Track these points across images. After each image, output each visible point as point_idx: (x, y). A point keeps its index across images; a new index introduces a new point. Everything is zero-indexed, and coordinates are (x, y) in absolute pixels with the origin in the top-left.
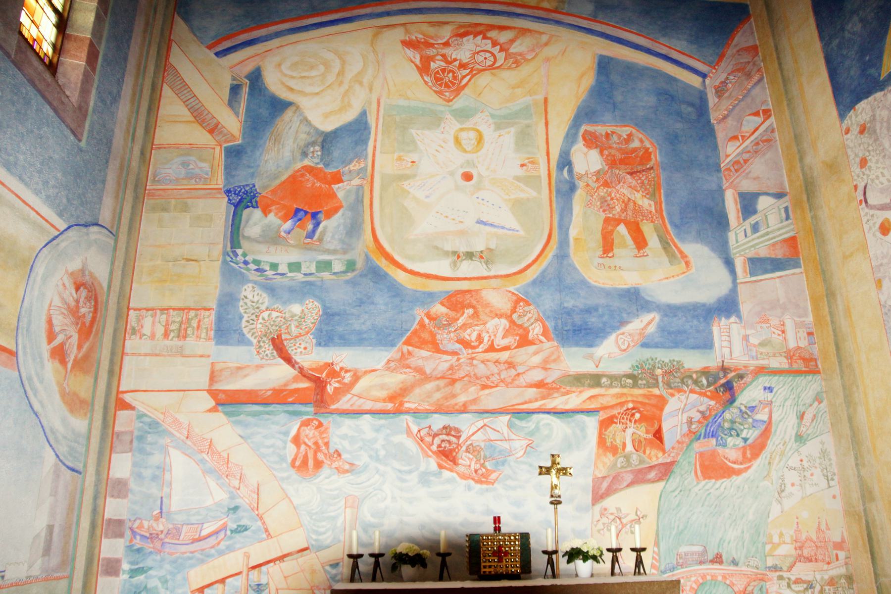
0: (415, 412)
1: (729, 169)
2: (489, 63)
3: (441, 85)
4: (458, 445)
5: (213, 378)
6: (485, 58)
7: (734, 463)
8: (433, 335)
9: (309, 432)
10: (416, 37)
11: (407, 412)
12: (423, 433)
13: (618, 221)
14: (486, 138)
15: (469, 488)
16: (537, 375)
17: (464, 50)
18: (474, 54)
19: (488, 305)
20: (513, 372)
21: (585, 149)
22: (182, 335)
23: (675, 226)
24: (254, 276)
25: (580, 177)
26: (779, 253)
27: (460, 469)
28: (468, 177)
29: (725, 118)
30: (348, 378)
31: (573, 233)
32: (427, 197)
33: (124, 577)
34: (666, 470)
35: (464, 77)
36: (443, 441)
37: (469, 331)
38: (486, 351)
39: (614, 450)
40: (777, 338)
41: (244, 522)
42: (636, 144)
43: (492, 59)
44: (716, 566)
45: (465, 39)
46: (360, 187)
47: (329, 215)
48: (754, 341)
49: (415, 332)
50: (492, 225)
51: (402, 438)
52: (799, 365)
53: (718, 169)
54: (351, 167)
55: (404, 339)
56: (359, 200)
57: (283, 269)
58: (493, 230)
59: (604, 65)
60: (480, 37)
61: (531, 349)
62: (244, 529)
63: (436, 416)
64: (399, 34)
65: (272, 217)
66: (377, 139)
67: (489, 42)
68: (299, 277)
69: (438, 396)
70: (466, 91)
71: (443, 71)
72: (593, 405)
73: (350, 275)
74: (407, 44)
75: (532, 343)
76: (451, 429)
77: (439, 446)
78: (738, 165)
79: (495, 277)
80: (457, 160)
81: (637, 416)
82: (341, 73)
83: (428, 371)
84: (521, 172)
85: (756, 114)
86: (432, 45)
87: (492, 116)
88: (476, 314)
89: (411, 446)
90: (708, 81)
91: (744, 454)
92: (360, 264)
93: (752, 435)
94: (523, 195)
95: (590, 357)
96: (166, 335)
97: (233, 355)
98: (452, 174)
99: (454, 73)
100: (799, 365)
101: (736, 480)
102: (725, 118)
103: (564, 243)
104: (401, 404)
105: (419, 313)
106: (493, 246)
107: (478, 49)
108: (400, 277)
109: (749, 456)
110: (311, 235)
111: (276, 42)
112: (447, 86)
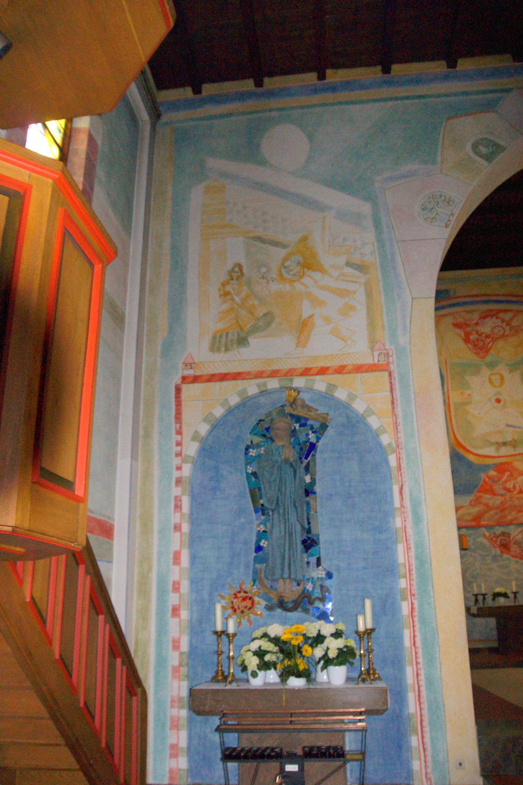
0: (486, 526)
2: (501, 333)
3: (477, 349)
4: (510, 542)
6: (499, 331)
8: (491, 486)
10: (460, 321)
11: (483, 526)
12: (492, 536)
15: (517, 562)
17: (486, 328)
18: (493, 328)
19: (516, 470)
28: (498, 401)
32: (479, 414)
35: (489, 343)
36: (502, 540)
37: (509, 483)
38: (518, 493)
43: (503, 331)
45: (487, 320)
49: (482, 486)
50: (514, 427)
51: (481, 539)
55: (477, 489)
58: (515, 429)
60: (494, 318)
63: (497, 527)
67: (499, 320)
69: (497, 517)
71: (477, 340)
74: (456, 325)
76: (506, 533)
77: (500, 542)
79: (519, 454)
80: (491, 392)
83: (491, 505)
86: (468, 325)
87: (508, 365)
99: (483, 341)
104: (480, 522)
105: (483, 476)
106: (516, 438)
107: (494, 325)
108: (471, 458)
112: (481, 349)
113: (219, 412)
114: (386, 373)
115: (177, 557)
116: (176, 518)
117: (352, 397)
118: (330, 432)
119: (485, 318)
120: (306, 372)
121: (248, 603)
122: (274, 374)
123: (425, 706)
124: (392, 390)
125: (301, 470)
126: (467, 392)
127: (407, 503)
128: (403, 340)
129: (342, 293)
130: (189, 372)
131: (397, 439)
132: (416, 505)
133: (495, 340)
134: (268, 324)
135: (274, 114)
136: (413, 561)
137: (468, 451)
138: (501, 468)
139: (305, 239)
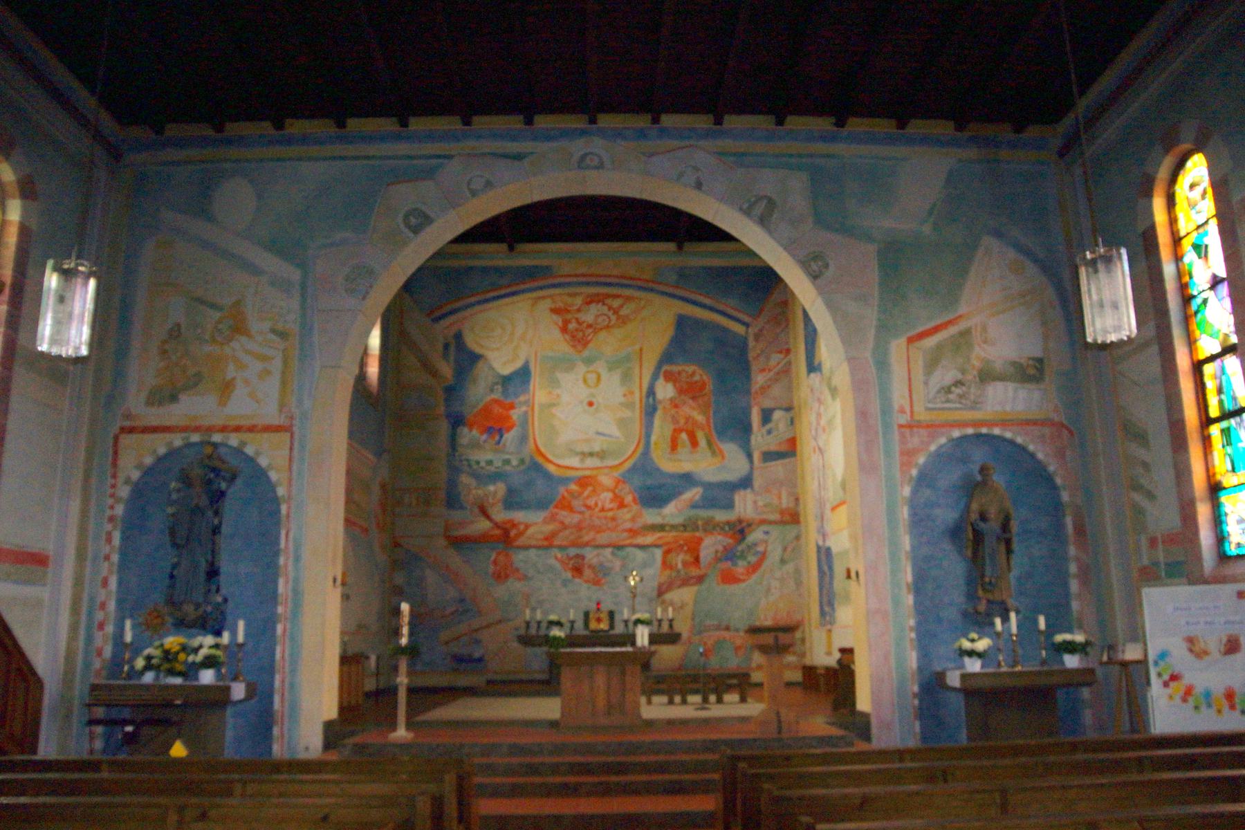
0: (561, 547)
1: (756, 393)
5: (447, 528)
7: (743, 574)
9: (502, 558)
13: (681, 430)
16: (628, 525)
17: (589, 315)
20: (614, 523)
21: (664, 383)
23: (718, 432)
25: (660, 402)
26: (784, 448)
27: (585, 578)
29: (758, 356)
30: (522, 527)
31: (654, 438)
34: (700, 579)
35: (589, 335)
39: (671, 568)
40: (776, 501)
42: (697, 378)
44: (726, 632)
46: (526, 413)
47: (509, 429)
48: (760, 503)
51: (552, 561)
52: (787, 518)
53: (748, 392)
54: (522, 398)
57: (483, 464)
58: (604, 438)
59: (681, 322)
60: (601, 304)
61: (625, 510)
62: (467, 611)
64: (548, 304)
65: (475, 432)
66: (536, 381)
68: (492, 469)
69: (572, 537)
71: (577, 330)
72: (661, 542)
74: (555, 311)
78: (764, 389)
79: (607, 467)
80: (583, 393)
81: (685, 548)
82: (512, 334)
84: (622, 399)
85: (780, 352)
86: (568, 311)
87: (607, 362)
89: (558, 565)
90: (750, 330)
91: (748, 571)
92: (527, 460)
93: (753, 559)
95: (659, 514)
97: (457, 515)
100: (787, 518)
101: (743, 585)
102: (758, 356)
103: (648, 443)
105: (562, 490)
106: (605, 447)
107: (599, 313)
109: (750, 571)
110: (498, 443)
111: (469, 311)
113: (148, 461)
114: (289, 434)
115: (105, 583)
116: (107, 549)
117: (258, 453)
118: (239, 482)
119: (588, 303)
120: (224, 429)
121: (159, 620)
122: (197, 429)
123: (286, 704)
124: (291, 449)
125: (210, 513)
126: (558, 391)
127: (291, 544)
129: (264, 358)
130: (127, 423)
132: (298, 547)
133: (596, 331)
134: (196, 385)
135: (227, 165)
136: (290, 594)
137: (550, 462)
138: (584, 482)
139: (238, 304)
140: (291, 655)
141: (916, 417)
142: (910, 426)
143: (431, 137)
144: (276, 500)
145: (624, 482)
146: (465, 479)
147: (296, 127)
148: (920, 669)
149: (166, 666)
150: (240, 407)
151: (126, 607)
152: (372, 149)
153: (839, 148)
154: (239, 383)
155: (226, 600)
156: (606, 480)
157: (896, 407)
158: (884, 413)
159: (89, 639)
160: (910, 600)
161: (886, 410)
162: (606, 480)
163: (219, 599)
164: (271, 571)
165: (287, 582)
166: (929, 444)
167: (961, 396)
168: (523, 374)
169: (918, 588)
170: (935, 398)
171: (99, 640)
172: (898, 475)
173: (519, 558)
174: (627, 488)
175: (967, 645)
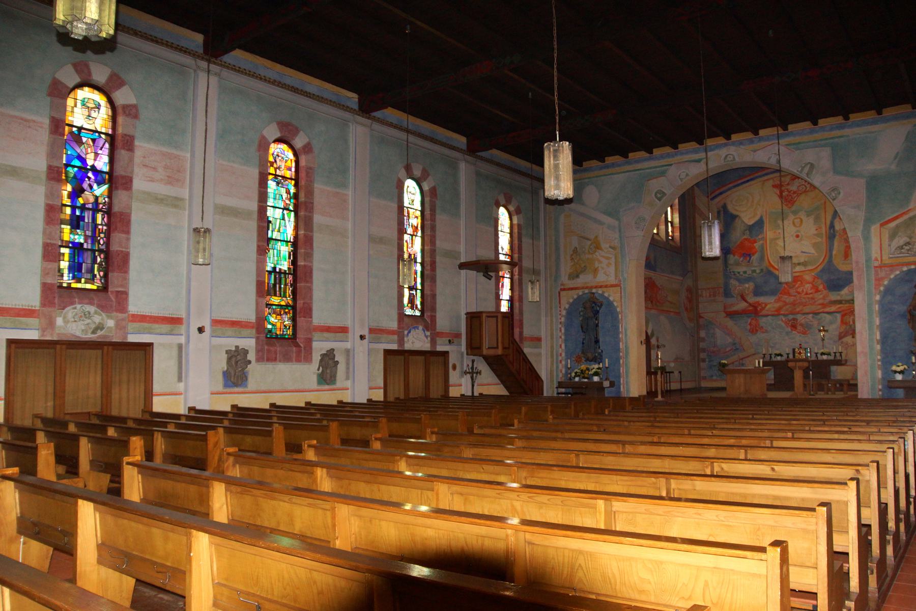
0: (784, 315)
5: (725, 307)
9: (753, 321)
11: (781, 314)
14: (804, 221)
16: (821, 301)
22: (715, 296)
24: (733, 276)
30: (763, 305)
31: (834, 252)
33: (707, 363)
39: (846, 324)
41: (738, 347)
47: (754, 254)
51: (780, 322)
54: (760, 237)
56: (763, 248)
62: (737, 349)
64: (771, 182)
65: (736, 257)
66: (767, 226)
68: (747, 275)
70: (796, 203)
72: (840, 310)
73: (762, 274)
74: (774, 186)
75: (820, 291)
82: (753, 201)
84: (816, 232)
88: (802, 283)
89: (783, 324)
94: (817, 241)
95: (839, 295)
96: (710, 296)
97: (730, 301)
98: (792, 236)
106: (806, 260)
110: (749, 262)
111: (729, 192)
112: (789, 202)
113: (571, 301)
116: (560, 334)
117: (609, 295)
118: (603, 307)
120: (596, 287)
122: (587, 288)
125: (594, 320)
128: (625, 275)
129: (608, 258)
130: (562, 287)
131: (622, 309)
134: (585, 270)
135: (586, 180)
139: (596, 237)
140: (626, 372)
141: (883, 262)
142: (880, 267)
143: (662, 157)
144: (617, 313)
145: (818, 278)
146: (733, 282)
147: (609, 160)
148: (883, 378)
149: (582, 375)
150: (601, 278)
151: (569, 355)
152: (639, 166)
153: (846, 131)
154: (600, 268)
155: (602, 351)
156: (808, 278)
157: (873, 258)
158: (867, 261)
159: (557, 367)
160: (879, 347)
161: (868, 260)
162: (808, 278)
163: (600, 351)
164: (617, 340)
165: (623, 344)
166: (890, 275)
167: (908, 250)
168: (760, 224)
169: (884, 341)
170: (894, 252)
171: (560, 366)
172: (874, 290)
173: (763, 321)
174: (819, 281)
175: (894, 368)
